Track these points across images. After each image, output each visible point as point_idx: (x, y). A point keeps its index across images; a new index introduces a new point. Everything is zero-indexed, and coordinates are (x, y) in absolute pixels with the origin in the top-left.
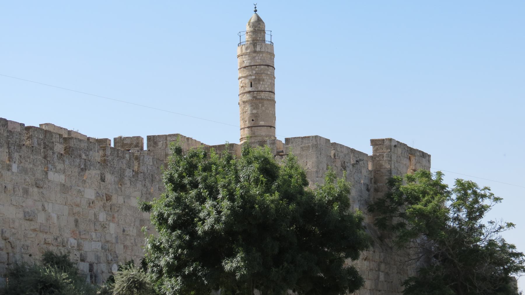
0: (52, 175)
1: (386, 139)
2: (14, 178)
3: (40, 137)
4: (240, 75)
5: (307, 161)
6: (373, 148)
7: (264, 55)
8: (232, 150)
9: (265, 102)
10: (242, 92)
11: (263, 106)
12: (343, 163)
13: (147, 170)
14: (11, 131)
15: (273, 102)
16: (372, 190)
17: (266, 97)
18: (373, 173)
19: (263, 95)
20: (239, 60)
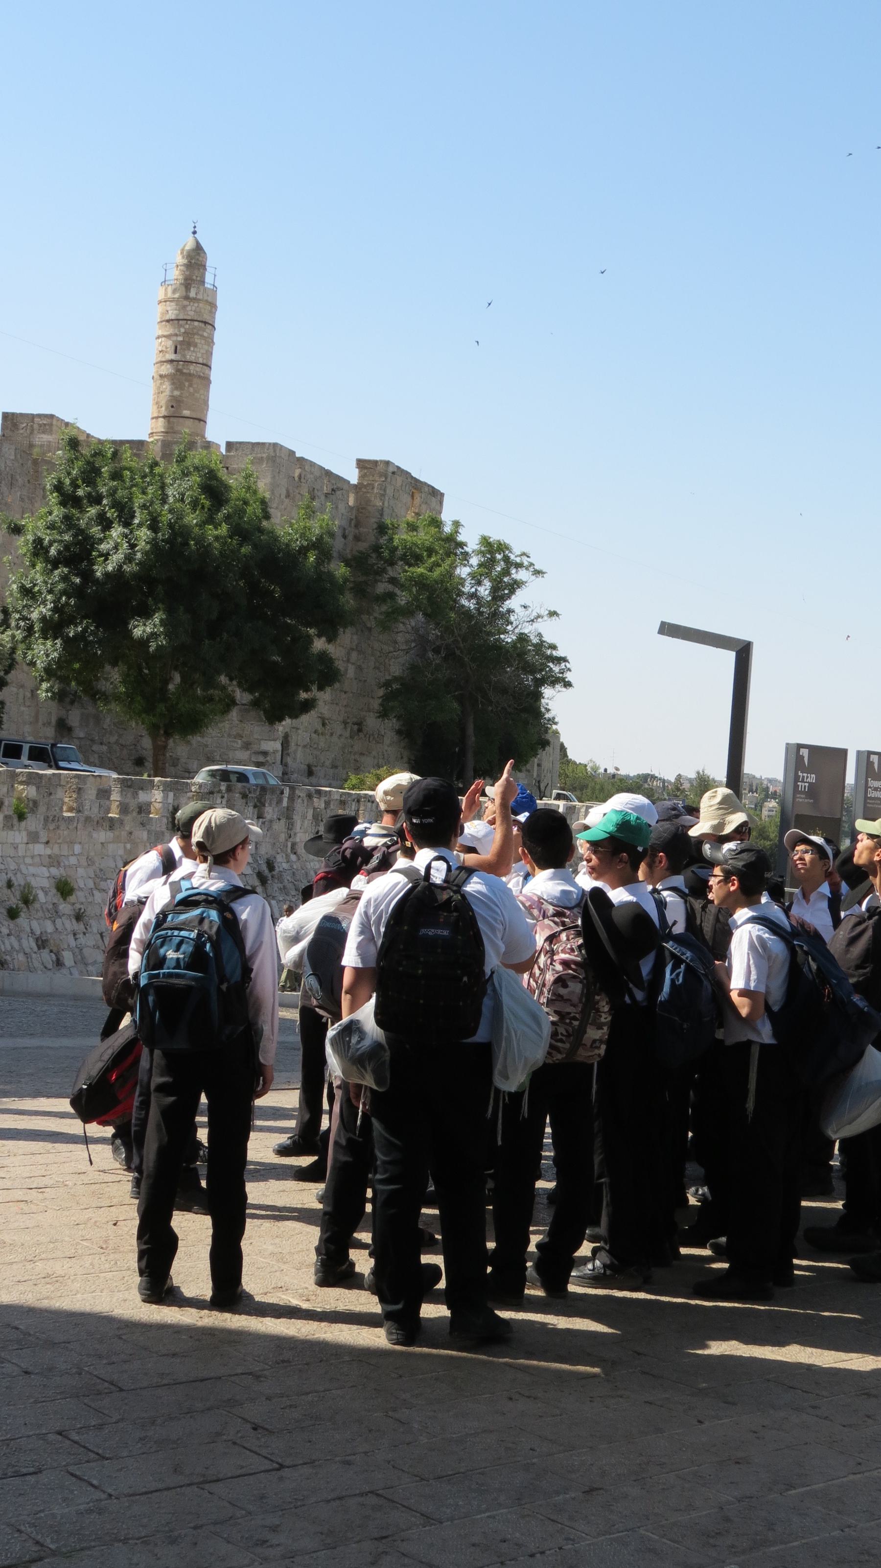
1: (381, 461)
4: (160, 333)
6: (360, 472)
7: (201, 305)
8: (141, 450)
9: (195, 380)
10: (159, 359)
11: (191, 385)
12: (311, 489)
13: (6, 467)
15: (206, 381)
16: (350, 537)
17: (197, 372)
18: (354, 512)
19: (192, 368)
20: (160, 309)
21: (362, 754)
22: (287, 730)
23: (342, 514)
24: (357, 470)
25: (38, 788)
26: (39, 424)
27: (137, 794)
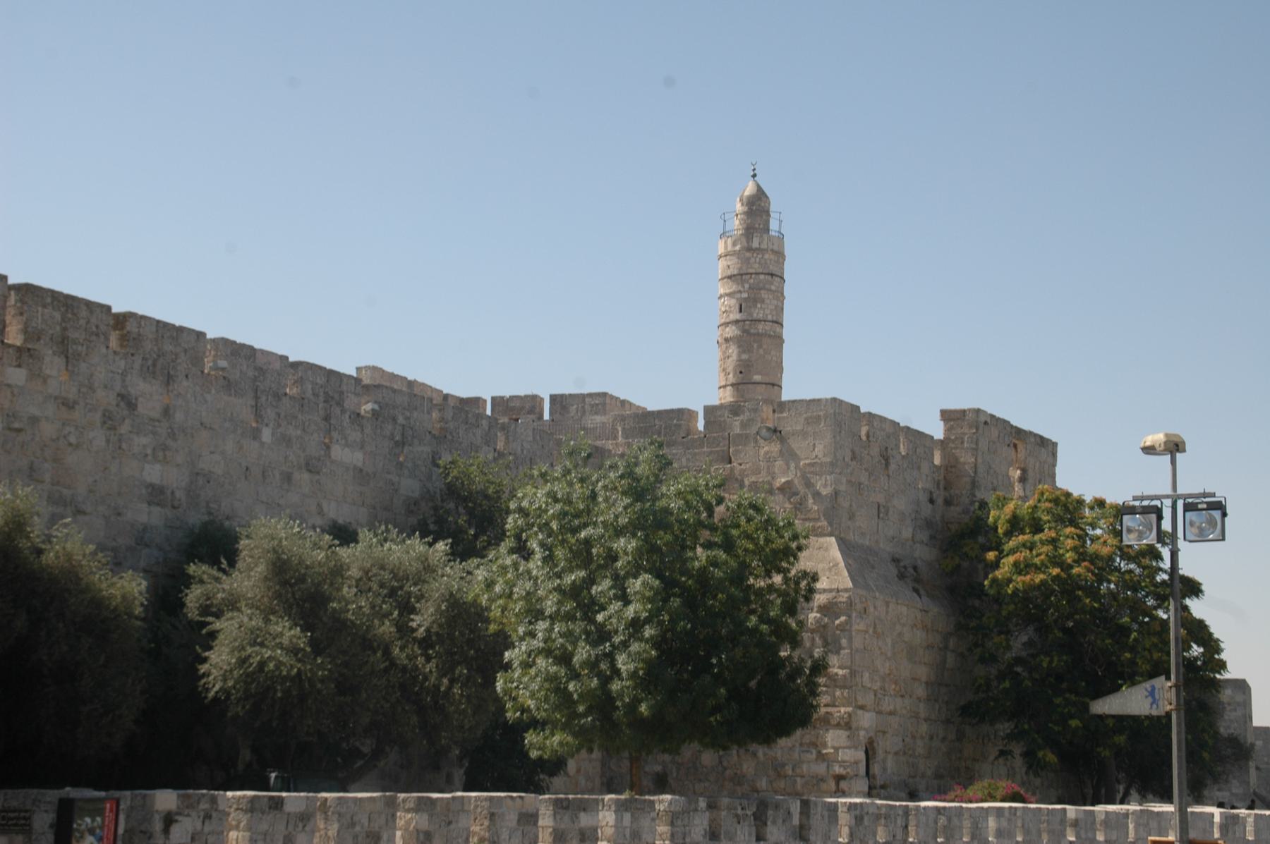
0: (338, 452)
1: (969, 410)
2: (265, 453)
3: (318, 381)
4: (722, 291)
5: (814, 444)
6: (945, 425)
10: (723, 321)
11: (760, 346)
13: (522, 450)
14: (261, 369)
15: (778, 340)
16: (940, 501)
18: (942, 470)
19: (760, 327)
20: (722, 264)
21: (974, 760)
22: (872, 734)
23: (927, 476)
24: (942, 422)
25: (431, 816)
26: (590, 405)
27: (577, 818)
